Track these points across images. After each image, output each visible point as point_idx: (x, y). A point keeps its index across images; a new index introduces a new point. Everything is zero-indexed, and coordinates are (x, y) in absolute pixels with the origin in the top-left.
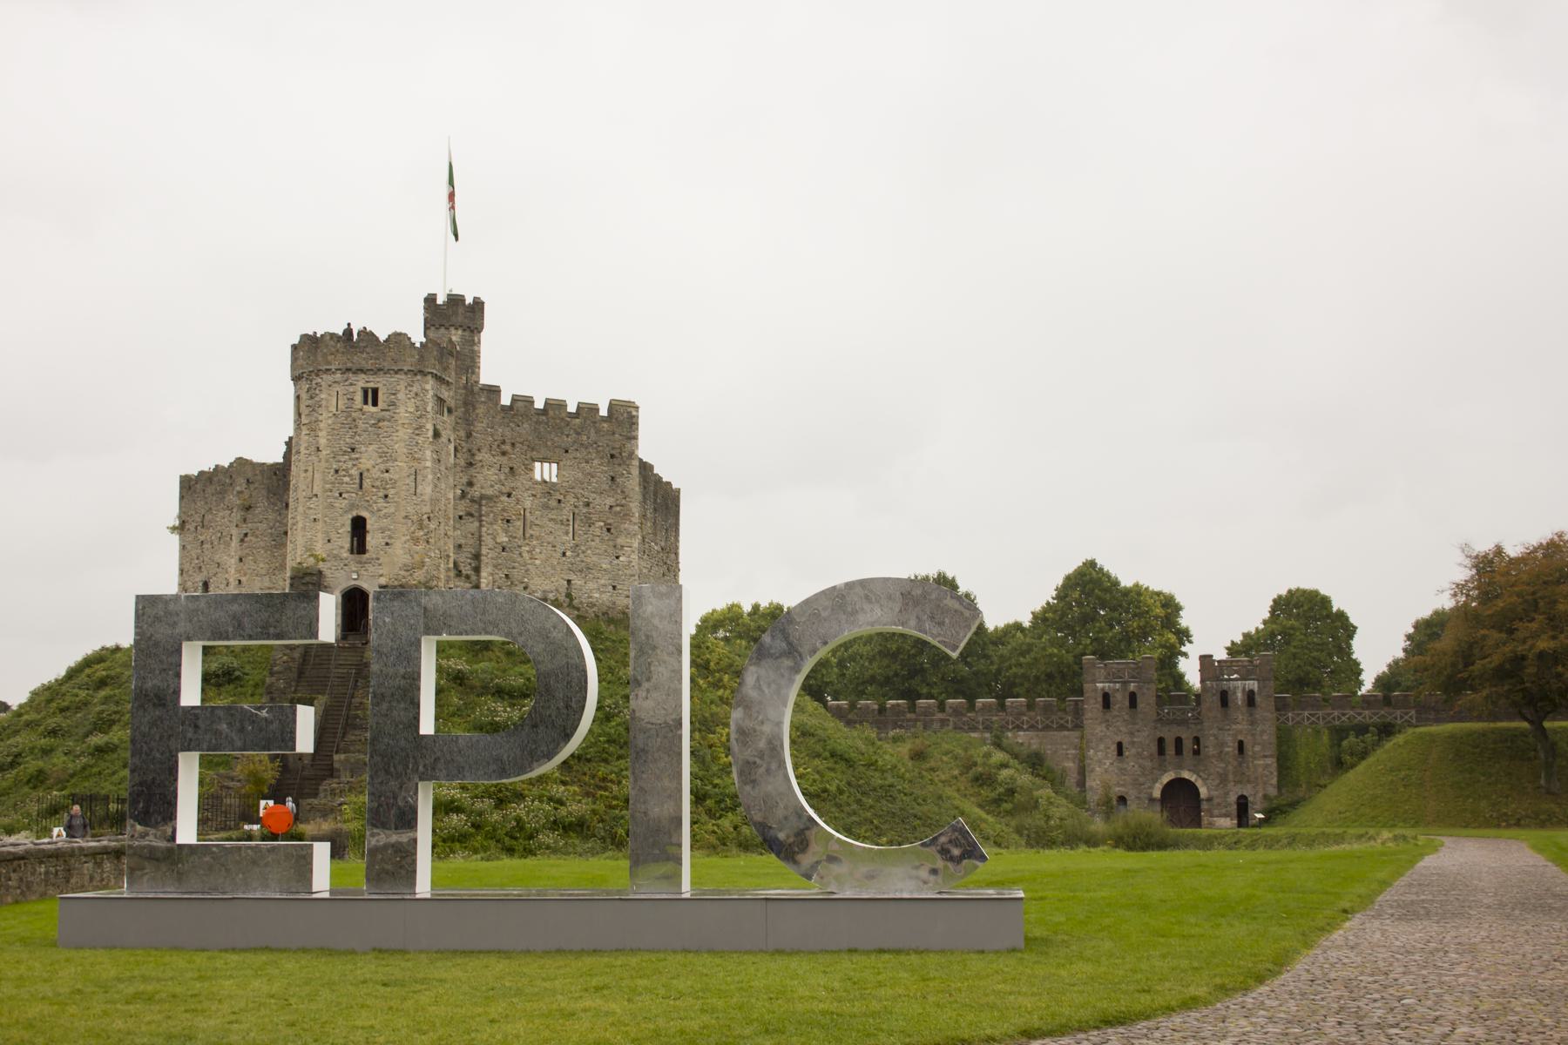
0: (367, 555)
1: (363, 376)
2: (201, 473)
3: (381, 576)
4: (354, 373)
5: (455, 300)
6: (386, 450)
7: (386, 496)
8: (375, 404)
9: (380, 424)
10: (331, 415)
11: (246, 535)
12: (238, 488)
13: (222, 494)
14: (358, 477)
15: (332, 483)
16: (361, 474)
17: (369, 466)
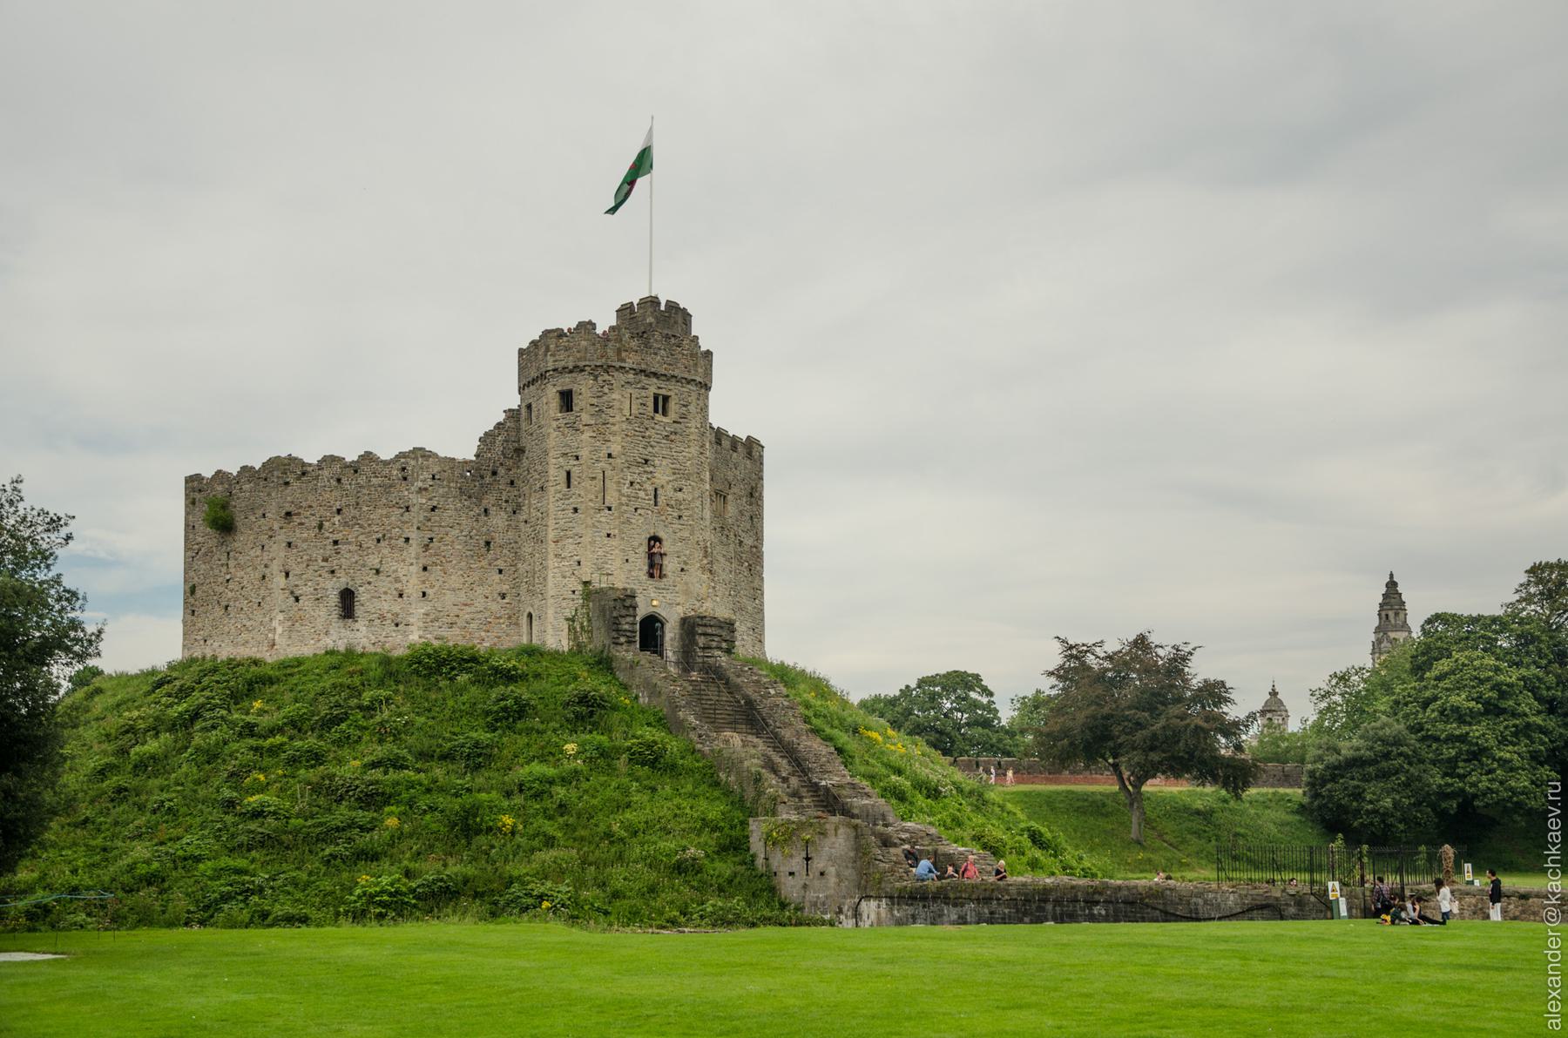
0: (664, 580)
1: (655, 380)
2: (329, 460)
3: (678, 604)
4: (646, 376)
5: (672, 306)
6: (678, 466)
7: (680, 517)
8: (665, 414)
9: (673, 437)
10: (624, 419)
11: (431, 539)
12: (420, 484)
13: (387, 488)
14: (653, 493)
15: (628, 496)
16: (656, 489)
17: (664, 483)
